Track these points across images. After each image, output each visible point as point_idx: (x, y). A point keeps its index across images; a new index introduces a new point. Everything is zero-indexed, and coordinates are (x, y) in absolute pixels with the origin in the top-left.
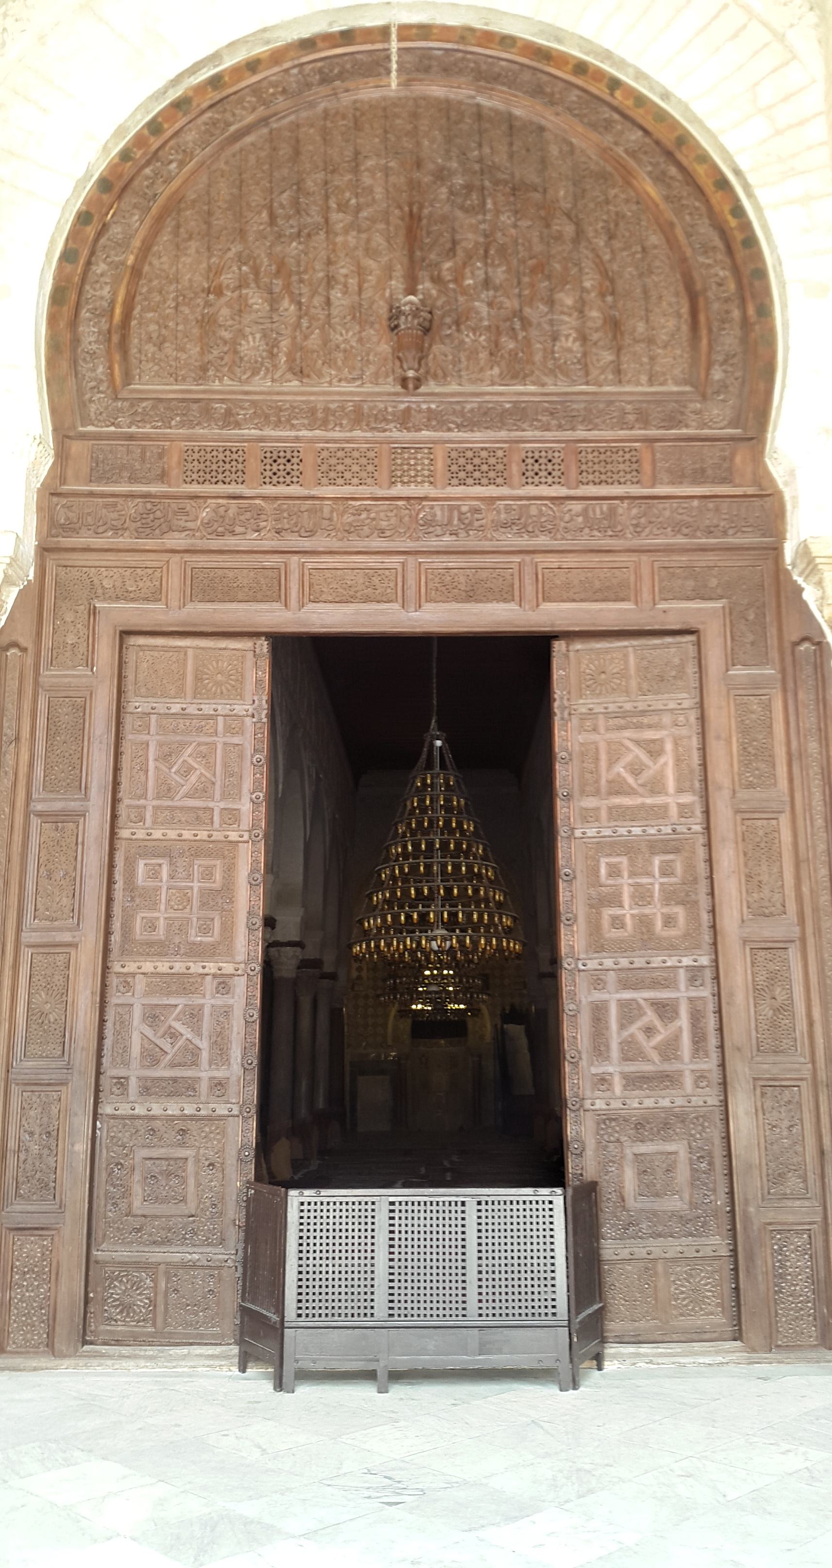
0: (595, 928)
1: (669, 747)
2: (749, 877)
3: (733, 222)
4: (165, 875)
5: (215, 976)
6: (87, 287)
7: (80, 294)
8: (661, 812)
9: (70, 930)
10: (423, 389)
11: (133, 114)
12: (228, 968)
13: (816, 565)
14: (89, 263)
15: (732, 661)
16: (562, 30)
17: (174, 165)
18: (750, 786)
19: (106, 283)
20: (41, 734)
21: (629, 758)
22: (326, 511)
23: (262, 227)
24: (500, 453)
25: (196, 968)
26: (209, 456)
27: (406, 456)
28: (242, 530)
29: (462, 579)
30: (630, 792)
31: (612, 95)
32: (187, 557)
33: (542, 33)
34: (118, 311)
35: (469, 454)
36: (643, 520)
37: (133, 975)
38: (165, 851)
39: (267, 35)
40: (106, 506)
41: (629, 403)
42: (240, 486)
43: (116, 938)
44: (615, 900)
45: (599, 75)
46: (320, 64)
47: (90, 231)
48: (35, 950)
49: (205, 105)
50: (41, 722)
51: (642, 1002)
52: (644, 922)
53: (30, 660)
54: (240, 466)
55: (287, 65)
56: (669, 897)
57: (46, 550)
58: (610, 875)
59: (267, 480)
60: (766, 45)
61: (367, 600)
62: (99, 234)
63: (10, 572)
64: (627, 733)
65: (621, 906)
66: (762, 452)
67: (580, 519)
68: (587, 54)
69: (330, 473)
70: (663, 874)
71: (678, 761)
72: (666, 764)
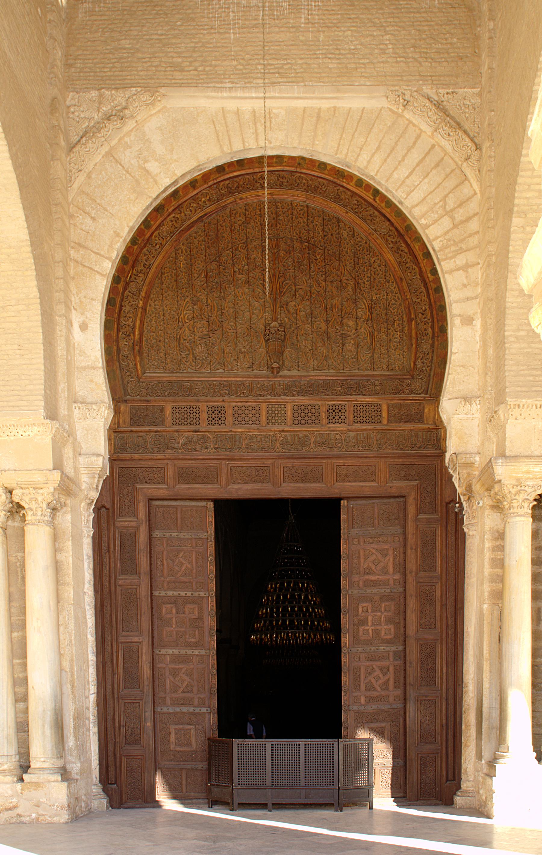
3: (431, 278)
5: (197, 655)
6: (121, 319)
7: (118, 324)
8: (385, 583)
9: (137, 636)
10: (280, 374)
12: (203, 652)
14: (121, 306)
15: (419, 510)
17: (158, 246)
18: (425, 570)
19: (130, 317)
21: (372, 558)
24: (317, 407)
25: (189, 652)
26: (183, 410)
29: (300, 471)
30: (374, 574)
31: (374, 200)
33: (339, 163)
34: (137, 333)
37: (165, 655)
38: (175, 601)
39: (199, 168)
40: (138, 437)
41: (378, 380)
42: (198, 426)
43: (156, 639)
45: (368, 187)
46: (227, 182)
47: (120, 287)
48: (125, 645)
49: (170, 210)
50: (117, 543)
54: (198, 415)
55: (211, 183)
56: (389, 621)
59: (210, 422)
61: (256, 482)
62: (125, 289)
64: (373, 546)
66: (438, 407)
68: (363, 175)
69: (238, 420)
71: (395, 558)
72: (389, 560)
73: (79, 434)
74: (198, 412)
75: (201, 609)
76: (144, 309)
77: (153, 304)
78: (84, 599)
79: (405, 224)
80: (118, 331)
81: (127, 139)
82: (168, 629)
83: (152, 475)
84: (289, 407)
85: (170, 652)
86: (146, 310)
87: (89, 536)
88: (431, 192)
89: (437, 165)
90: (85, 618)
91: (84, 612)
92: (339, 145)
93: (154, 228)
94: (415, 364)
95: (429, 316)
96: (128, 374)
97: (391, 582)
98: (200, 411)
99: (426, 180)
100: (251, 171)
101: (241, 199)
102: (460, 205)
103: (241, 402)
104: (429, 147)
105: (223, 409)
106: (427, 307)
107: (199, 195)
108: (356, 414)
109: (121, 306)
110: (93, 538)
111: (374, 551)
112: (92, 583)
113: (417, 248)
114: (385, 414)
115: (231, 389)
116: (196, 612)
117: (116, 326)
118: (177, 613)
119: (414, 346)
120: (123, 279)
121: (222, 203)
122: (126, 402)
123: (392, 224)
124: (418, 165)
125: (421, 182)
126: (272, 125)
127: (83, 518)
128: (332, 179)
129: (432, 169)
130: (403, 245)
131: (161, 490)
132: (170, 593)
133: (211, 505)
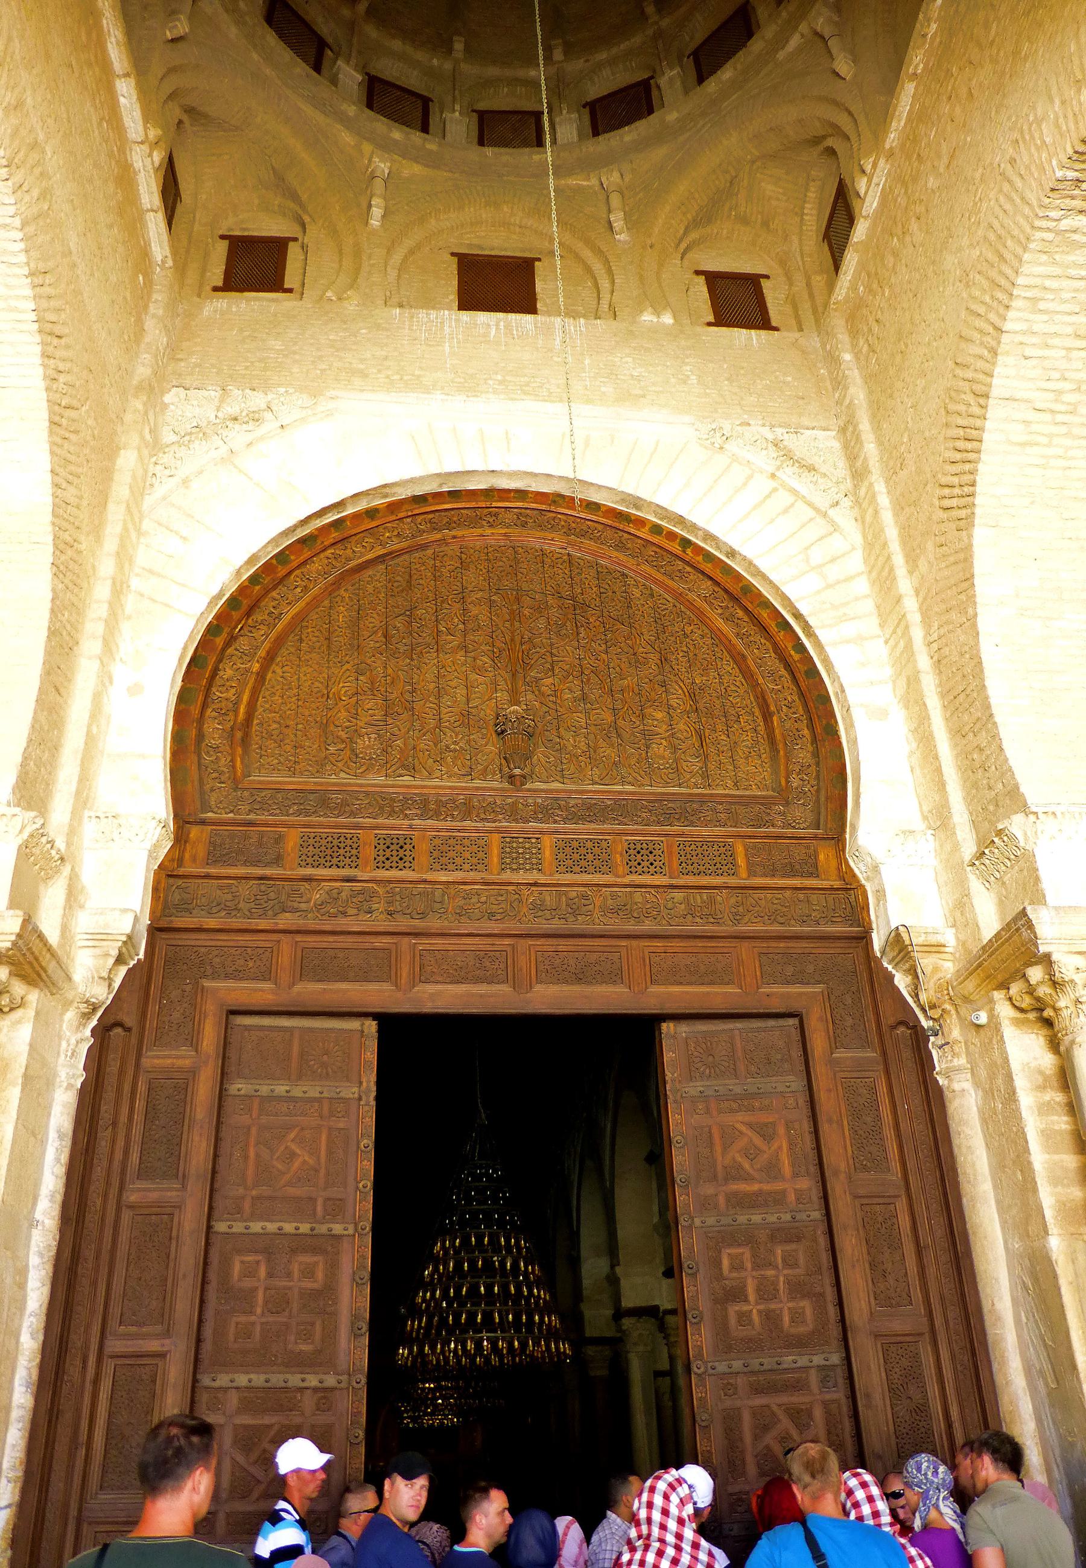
0: (722, 1329)
1: (781, 1130)
2: (873, 1266)
4: (262, 1272)
5: (315, 1390)
6: (214, 690)
9: (157, 1336)
11: (265, 546)
12: (330, 1381)
13: (909, 952)
15: (835, 1042)
16: (641, 499)
17: (299, 590)
18: (866, 1169)
20: (138, 1117)
22: (438, 893)
23: (378, 645)
25: (295, 1380)
26: (324, 842)
27: (515, 845)
28: (355, 911)
29: (572, 962)
30: (748, 1178)
31: (684, 552)
32: (299, 938)
33: (623, 501)
35: (575, 844)
36: (741, 909)
37: (225, 1390)
40: (220, 888)
41: (721, 803)
43: (207, 1346)
44: (736, 1294)
46: (431, 516)
47: (219, 641)
48: (120, 1362)
50: (140, 1105)
51: (775, 1408)
52: (771, 1319)
53: (134, 1041)
54: (354, 852)
56: (797, 1289)
57: (160, 930)
58: (733, 1268)
59: (380, 865)
60: (811, 519)
61: (478, 980)
62: (228, 644)
63: (124, 950)
64: (741, 1116)
65: (746, 1301)
67: (683, 906)
68: (661, 519)
70: (787, 1264)
71: (792, 1145)
72: (780, 1148)
73: (88, 876)
74: (355, 846)
75: (333, 1266)
76: (261, 677)
77: (279, 671)
78: (29, 1237)
79: (741, 585)
80: (204, 706)
82: (243, 1319)
83: (242, 962)
84: (547, 841)
85: (242, 1380)
86: (263, 678)
87: (70, 1086)
90: (22, 1286)
91: (22, 1273)
93: (295, 564)
94: (787, 782)
95: (801, 710)
96: (214, 775)
97: (791, 1197)
98: (361, 843)
100: (473, 505)
101: (454, 537)
103: (448, 830)
105: (408, 841)
106: (796, 698)
107: (381, 529)
108: (683, 859)
110: (83, 1092)
111: (743, 1129)
112: (59, 1198)
113: (765, 615)
114: (741, 861)
115: (429, 807)
116: (320, 1275)
117: (201, 698)
118: (270, 1275)
119: (782, 753)
120: (227, 630)
121: (422, 539)
122: (203, 822)
123: (717, 584)
127: (64, 1044)
128: (610, 522)
130: (738, 611)
131: (262, 993)
132: (256, 1227)
133: (371, 1026)
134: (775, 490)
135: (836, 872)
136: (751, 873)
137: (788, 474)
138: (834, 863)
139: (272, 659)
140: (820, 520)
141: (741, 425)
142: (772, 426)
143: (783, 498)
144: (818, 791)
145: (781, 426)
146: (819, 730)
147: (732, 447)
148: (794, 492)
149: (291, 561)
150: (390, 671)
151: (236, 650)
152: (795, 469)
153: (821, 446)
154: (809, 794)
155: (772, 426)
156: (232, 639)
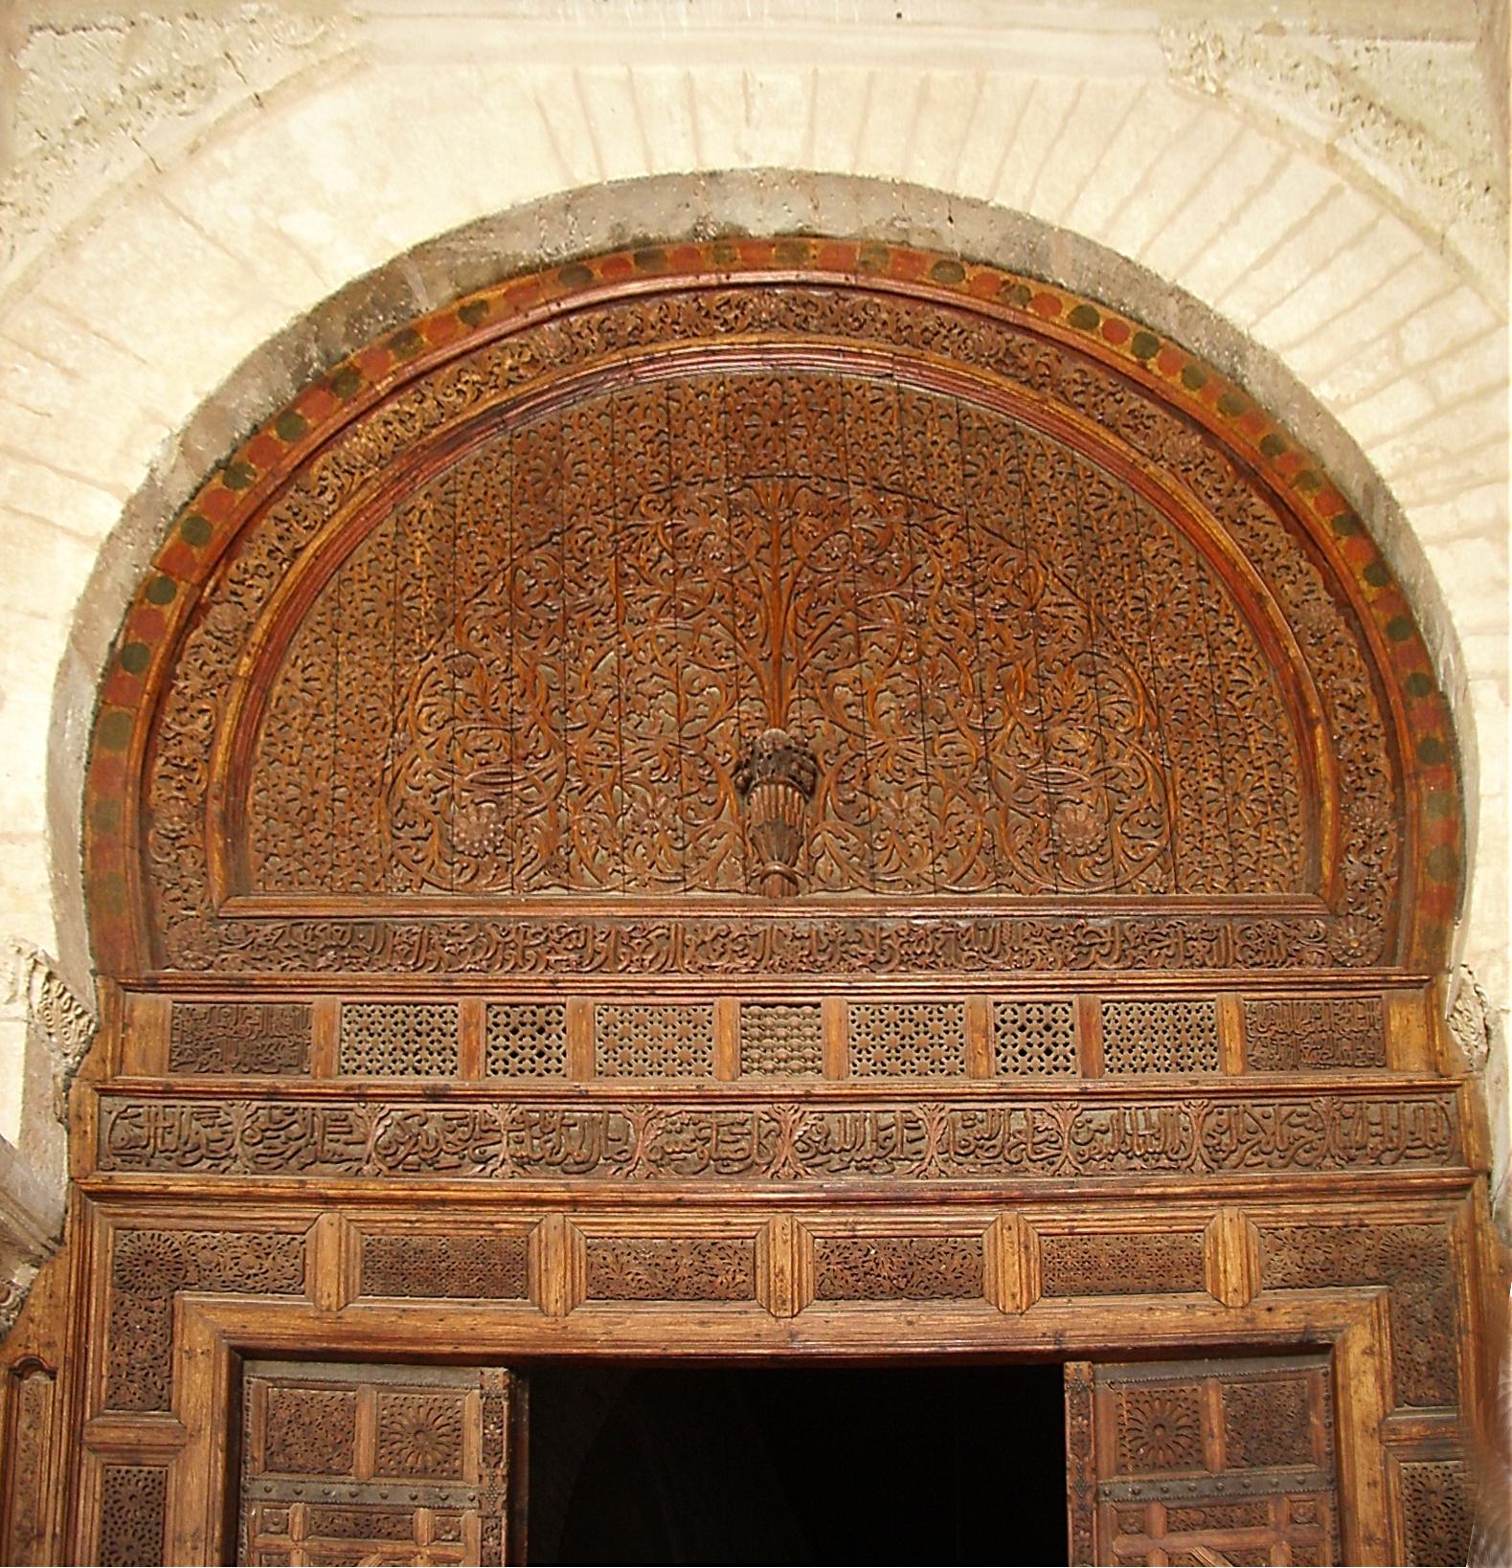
19: (203, 711)
36: (1225, 1139)
47: (171, 613)
60: (1411, 259)
81: (222, 155)
86: (266, 691)
88: (1345, 311)
89: (1356, 241)
92: (999, 173)
99: (1322, 278)
102: (1454, 351)
104: (1325, 192)
109: (167, 679)
119: (1328, 805)
120: (183, 587)
124: (1290, 235)
125: (1303, 283)
126: (755, 113)
129: (1339, 251)
134: (1335, 192)
135: (1423, 1055)
136: (1252, 1064)
137: (1362, 148)
138: (1418, 1035)
139: (281, 651)
140: (1431, 260)
141: (1264, 30)
142: (1334, 33)
143: (1357, 206)
144: (1398, 885)
145: (1351, 33)
146: (1408, 751)
147: (1243, 86)
148: (1375, 191)
149: (306, 432)
150: (517, 667)
151: (207, 632)
152: (1381, 128)
153: (1441, 80)
154: (1379, 894)
155: (1334, 33)
156: (195, 614)
